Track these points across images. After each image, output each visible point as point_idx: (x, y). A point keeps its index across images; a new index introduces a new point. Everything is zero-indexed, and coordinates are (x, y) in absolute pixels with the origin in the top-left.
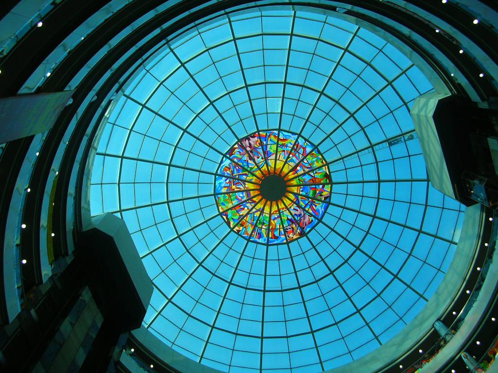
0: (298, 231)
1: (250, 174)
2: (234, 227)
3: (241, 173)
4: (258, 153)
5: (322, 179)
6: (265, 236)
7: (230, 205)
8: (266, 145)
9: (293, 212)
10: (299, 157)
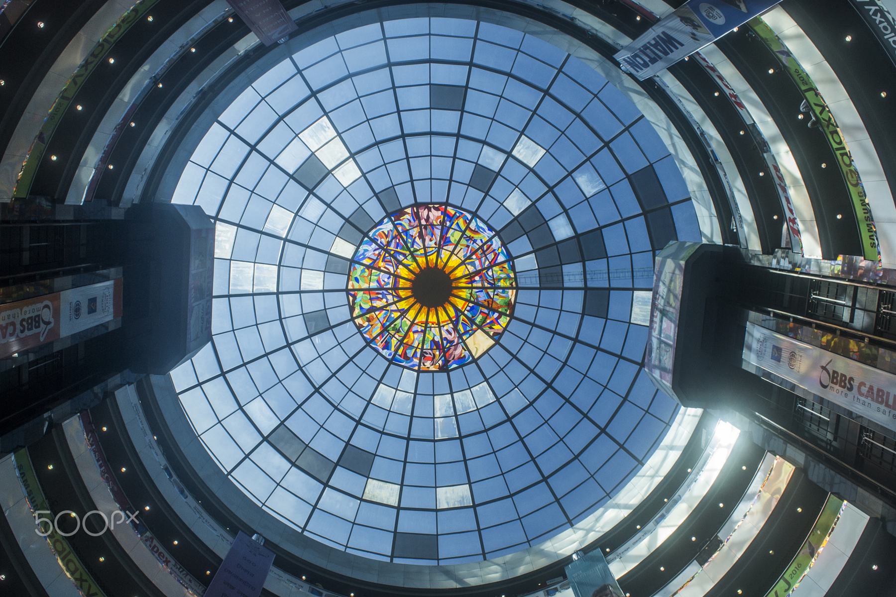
0: (440, 362)
1: (410, 256)
2: (357, 317)
3: (399, 250)
4: (433, 234)
5: (501, 306)
6: (393, 349)
7: (365, 286)
8: (450, 228)
9: (445, 335)
10: (484, 265)
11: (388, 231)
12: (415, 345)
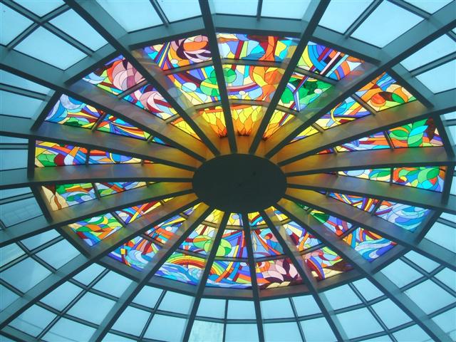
8: (239, 258)
11: (364, 240)
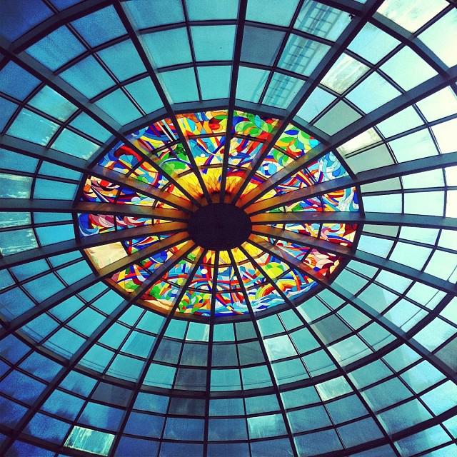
0: (94, 195)
6: (144, 138)
10: (219, 286)
12: (138, 171)
